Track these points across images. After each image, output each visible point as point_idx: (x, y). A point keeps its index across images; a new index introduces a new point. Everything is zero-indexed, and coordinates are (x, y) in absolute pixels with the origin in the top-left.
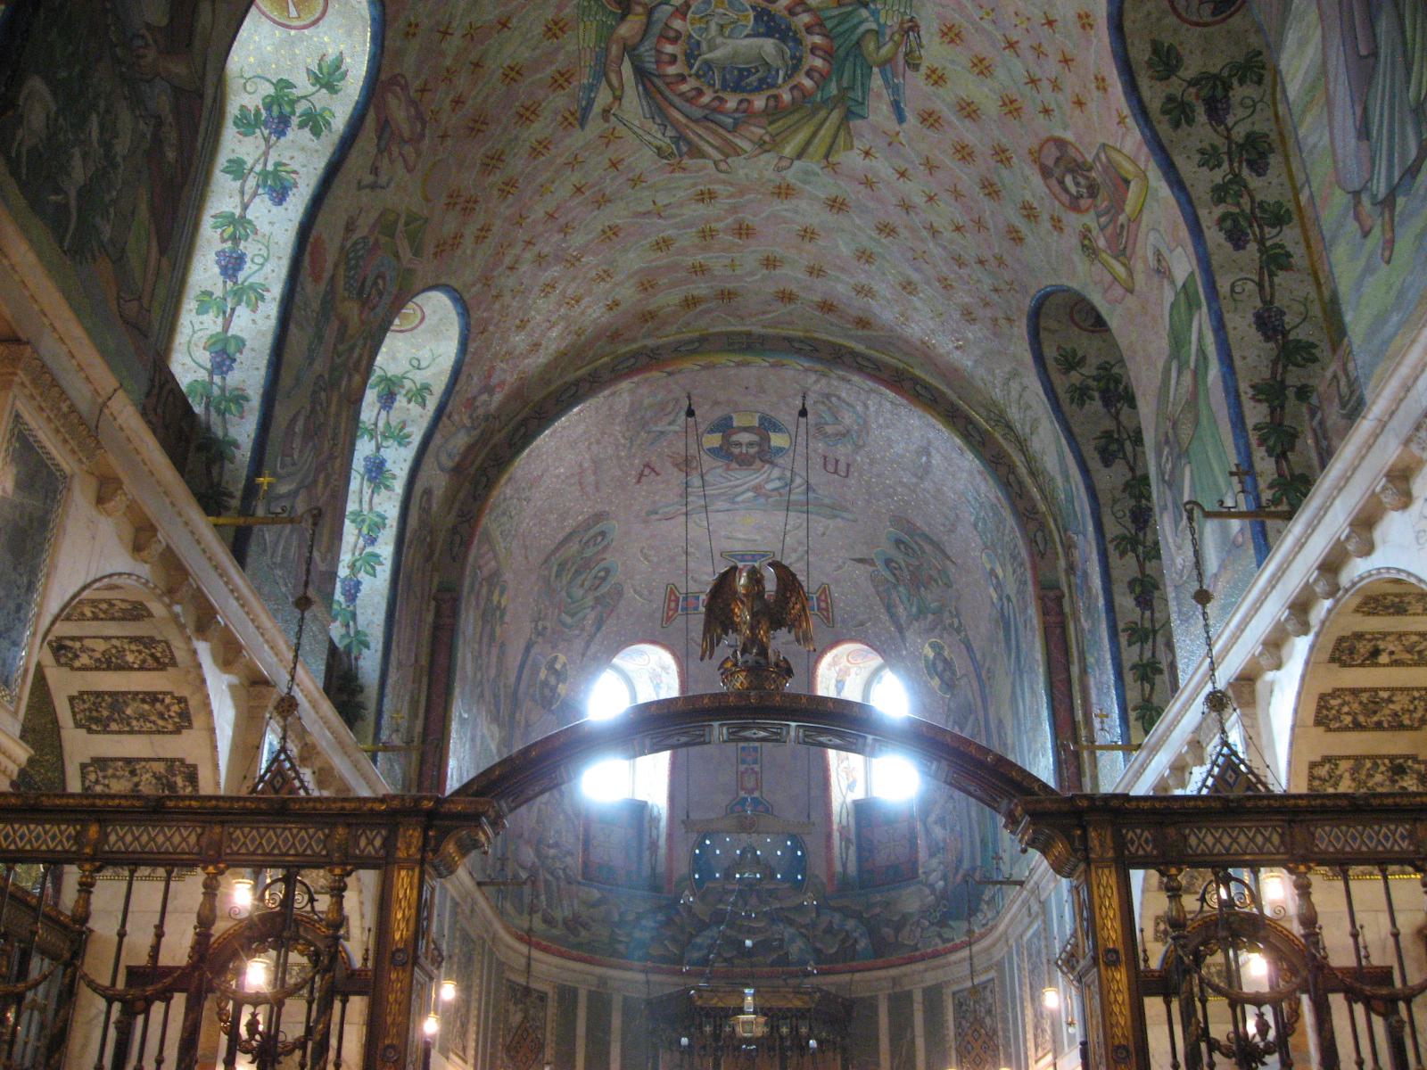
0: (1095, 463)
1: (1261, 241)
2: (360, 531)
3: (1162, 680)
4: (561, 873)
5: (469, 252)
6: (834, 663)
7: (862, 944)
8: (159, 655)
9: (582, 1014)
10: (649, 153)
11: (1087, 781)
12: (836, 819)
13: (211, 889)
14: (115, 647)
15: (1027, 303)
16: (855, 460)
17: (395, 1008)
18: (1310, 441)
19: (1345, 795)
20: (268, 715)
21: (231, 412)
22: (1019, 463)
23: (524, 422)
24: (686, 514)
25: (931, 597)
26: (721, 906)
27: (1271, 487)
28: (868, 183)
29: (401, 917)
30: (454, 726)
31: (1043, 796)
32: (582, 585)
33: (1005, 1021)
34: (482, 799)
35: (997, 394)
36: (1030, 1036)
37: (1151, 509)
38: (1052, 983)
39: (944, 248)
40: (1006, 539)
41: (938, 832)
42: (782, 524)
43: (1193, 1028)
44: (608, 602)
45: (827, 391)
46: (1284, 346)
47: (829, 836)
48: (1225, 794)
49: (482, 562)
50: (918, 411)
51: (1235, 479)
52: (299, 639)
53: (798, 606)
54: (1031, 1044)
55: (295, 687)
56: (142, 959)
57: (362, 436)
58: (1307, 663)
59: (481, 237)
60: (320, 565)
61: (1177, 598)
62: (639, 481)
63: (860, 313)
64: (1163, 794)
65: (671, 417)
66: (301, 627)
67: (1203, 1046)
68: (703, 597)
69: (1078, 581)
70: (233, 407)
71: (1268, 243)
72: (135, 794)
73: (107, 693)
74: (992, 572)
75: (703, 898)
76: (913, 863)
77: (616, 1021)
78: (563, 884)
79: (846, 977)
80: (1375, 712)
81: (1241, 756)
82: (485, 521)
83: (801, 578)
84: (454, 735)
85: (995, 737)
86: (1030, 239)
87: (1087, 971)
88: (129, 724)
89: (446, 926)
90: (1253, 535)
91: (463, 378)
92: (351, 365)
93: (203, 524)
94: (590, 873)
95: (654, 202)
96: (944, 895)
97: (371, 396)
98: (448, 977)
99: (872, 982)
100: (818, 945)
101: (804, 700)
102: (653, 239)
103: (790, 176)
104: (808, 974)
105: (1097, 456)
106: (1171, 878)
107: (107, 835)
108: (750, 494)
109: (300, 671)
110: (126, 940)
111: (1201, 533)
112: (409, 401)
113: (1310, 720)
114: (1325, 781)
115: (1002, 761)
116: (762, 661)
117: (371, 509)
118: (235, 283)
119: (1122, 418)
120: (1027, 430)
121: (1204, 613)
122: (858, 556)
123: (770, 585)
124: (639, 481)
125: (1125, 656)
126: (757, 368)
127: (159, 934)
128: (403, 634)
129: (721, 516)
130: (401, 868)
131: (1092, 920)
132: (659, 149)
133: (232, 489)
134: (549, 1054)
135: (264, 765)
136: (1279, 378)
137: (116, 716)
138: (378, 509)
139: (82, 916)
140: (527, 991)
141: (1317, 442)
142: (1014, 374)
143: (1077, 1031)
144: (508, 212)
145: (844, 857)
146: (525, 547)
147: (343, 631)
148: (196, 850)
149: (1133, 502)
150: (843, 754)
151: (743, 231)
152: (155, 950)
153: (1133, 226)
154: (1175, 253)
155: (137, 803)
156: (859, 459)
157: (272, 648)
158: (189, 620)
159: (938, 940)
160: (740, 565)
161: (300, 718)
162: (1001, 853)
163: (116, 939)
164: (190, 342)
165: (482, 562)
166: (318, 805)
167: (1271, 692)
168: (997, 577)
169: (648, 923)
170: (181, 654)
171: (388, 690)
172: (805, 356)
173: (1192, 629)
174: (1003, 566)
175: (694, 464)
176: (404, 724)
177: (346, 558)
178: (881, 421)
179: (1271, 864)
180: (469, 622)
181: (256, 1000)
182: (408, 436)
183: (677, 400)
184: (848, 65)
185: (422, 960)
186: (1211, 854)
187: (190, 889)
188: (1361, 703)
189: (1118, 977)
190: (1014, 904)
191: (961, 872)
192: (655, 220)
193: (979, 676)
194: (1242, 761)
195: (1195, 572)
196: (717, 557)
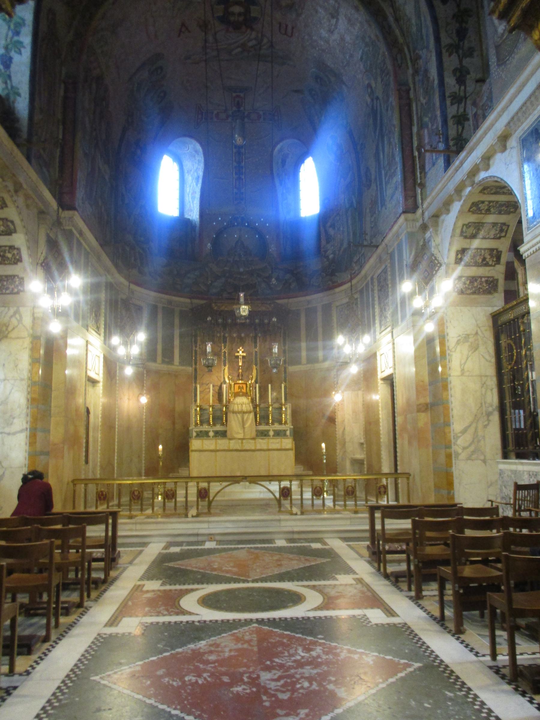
22: (388, 14)
74: (369, 86)
125: (449, 110)
149: (458, 25)
168: (371, 87)
191: (342, 249)
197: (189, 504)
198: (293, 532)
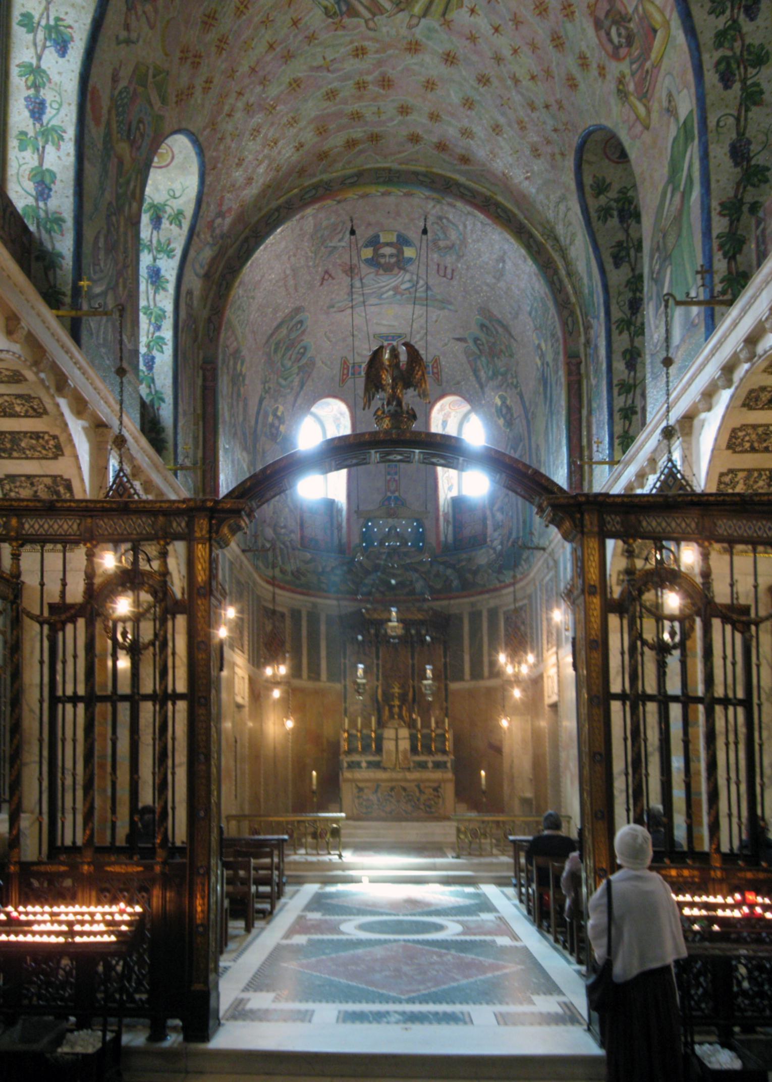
0: (609, 266)
1: (744, 81)
2: (150, 321)
3: (636, 418)
4: (288, 543)
5: (199, 101)
6: (442, 409)
7: (455, 583)
8: (36, 407)
9: (304, 624)
10: (319, 13)
11: (586, 484)
12: (441, 509)
13: (90, 556)
14: (7, 401)
15: (576, 141)
16: (457, 267)
17: (202, 620)
18: (753, 246)
19: (739, 494)
20: (109, 447)
21: (55, 232)
22: (561, 267)
23: (246, 239)
24: (352, 307)
25: (501, 363)
26: (378, 561)
27: (721, 282)
28: (472, 38)
29: (200, 567)
30: (221, 453)
31: (559, 495)
32: (290, 359)
33: (531, 628)
34: (241, 501)
35: (550, 215)
36: (545, 637)
37: (641, 299)
38: (558, 607)
39: (522, 95)
40: (549, 322)
41: (499, 516)
42: (411, 314)
43: (634, 633)
44: (306, 369)
45: (440, 214)
46: (747, 170)
47: (437, 519)
48: (666, 493)
49: (228, 343)
50: (499, 229)
51: (699, 276)
52: (121, 396)
53: (420, 373)
54: (545, 642)
55: (124, 429)
56: (56, 599)
57: (143, 250)
58: (727, 407)
59: (206, 90)
60: (128, 346)
61: (652, 363)
62: (322, 284)
63: (463, 152)
64: (630, 493)
65: (340, 236)
66: (121, 388)
67: (639, 643)
68: (364, 365)
69: (592, 351)
70: (56, 227)
71: (749, 82)
72: (36, 498)
73: (6, 432)
74: (539, 346)
75: (367, 557)
76: (485, 535)
77: (323, 628)
78: (290, 550)
79: (445, 603)
80: (765, 441)
81: (679, 468)
82: (229, 314)
83: (422, 352)
84: (221, 459)
85: (534, 456)
86: (582, 87)
87: (578, 597)
88: (24, 453)
89: (227, 575)
90: (706, 317)
91: (204, 206)
92: (129, 193)
93: (49, 314)
94: (305, 543)
95: (324, 58)
96: (500, 554)
97: (145, 219)
98: (231, 604)
99: (460, 605)
100: (431, 583)
101: (423, 436)
102: (323, 90)
103: (418, 33)
104: (425, 600)
105: (611, 260)
106: (630, 545)
107: (23, 524)
108: (391, 293)
109: (125, 419)
110: (45, 587)
111: (672, 318)
112: (171, 224)
113: (724, 445)
114: (727, 484)
115: (537, 473)
116: (399, 410)
117: (155, 305)
118: (42, 125)
119: (631, 231)
120: (568, 242)
121: (667, 373)
122: (458, 336)
123: (403, 357)
124: (322, 284)
125: (615, 402)
126: (395, 197)
127: (64, 584)
128: (184, 393)
129: (373, 309)
130: (198, 543)
131: (582, 568)
132: (326, 8)
133: (64, 290)
134: (288, 646)
135: (111, 480)
136: (739, 197)
137: (15, 447)
138: (160, 305)
139: (17, 574)
140: (274, 612)
141: (758, 246)
142: (563, 198)
143: (570, 634)
144: (223, 67)
145: (445, 531)
146: (253, 332)
147: (147, 391)
148: (78, 533)
150: (446, 469)
151: (386, 83)
152: (63, 593)
153: (655, 71)
154: (682, 94)
155: (38, 504)
156: (459, 265)
157: (106, 402)
158: (51, 383)
159: (496, 582)
160: (385, 343)
161: (129, 449)
162: (534, 531)
163: (39, 587)
164: (18, 174)
165: (228, 343)
166: (147, 505)
167: (703, 426)
168: (541, 350)
169: (338, 572)
170: (49, 406)
171: (180, 430)
172: (426, 186)
173: (658, 384)
174: (546, 341)
175: (356, 271)
176: (191, 452)
177: (143, 340)
178: (474, 236)
179: (688, 539)
180: (224, 385)
181: (124, 620)
182: (173, 250)
183: (344, 223)
185: (215, 593)
186: (654, 532)
187: (78, 557)
188: (757, 434)
189: (595, 600)
190: (539, 561)
191: (511, 540)
192: (325, 73)
193: (527, 417)
194: (679, 471)
195: (665, 345)
196: (372, 338)
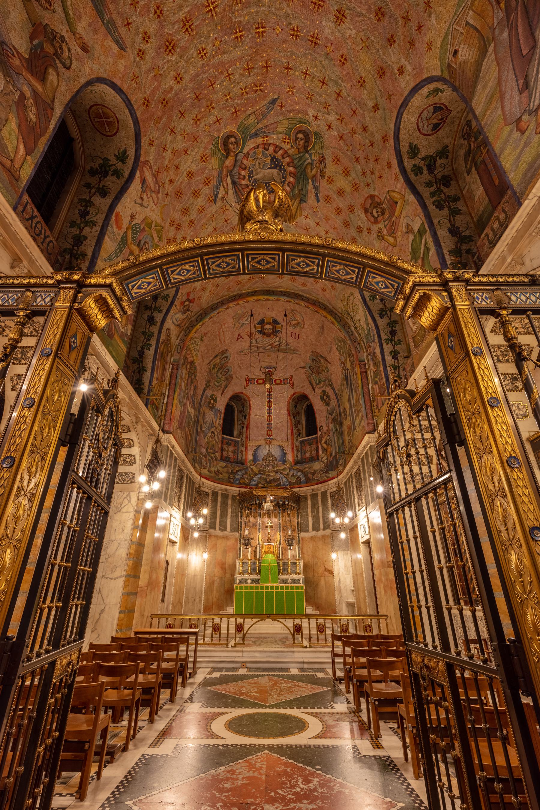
184: (301, 179)
197: (229, 636)
198: (303, 663)
